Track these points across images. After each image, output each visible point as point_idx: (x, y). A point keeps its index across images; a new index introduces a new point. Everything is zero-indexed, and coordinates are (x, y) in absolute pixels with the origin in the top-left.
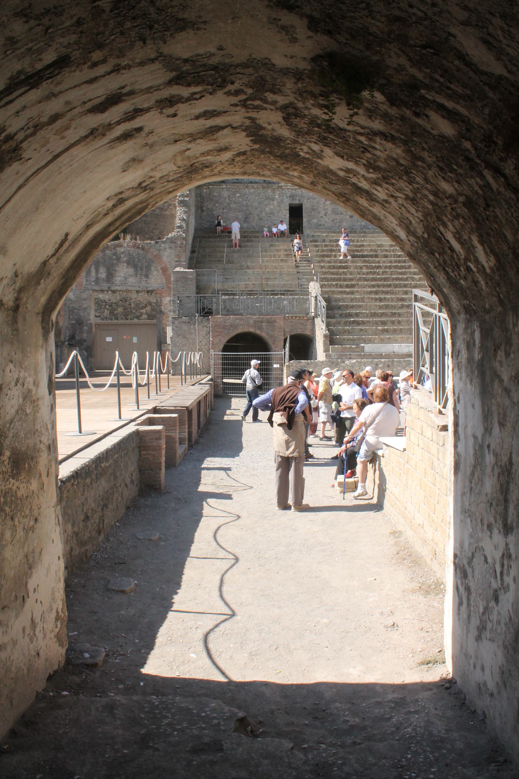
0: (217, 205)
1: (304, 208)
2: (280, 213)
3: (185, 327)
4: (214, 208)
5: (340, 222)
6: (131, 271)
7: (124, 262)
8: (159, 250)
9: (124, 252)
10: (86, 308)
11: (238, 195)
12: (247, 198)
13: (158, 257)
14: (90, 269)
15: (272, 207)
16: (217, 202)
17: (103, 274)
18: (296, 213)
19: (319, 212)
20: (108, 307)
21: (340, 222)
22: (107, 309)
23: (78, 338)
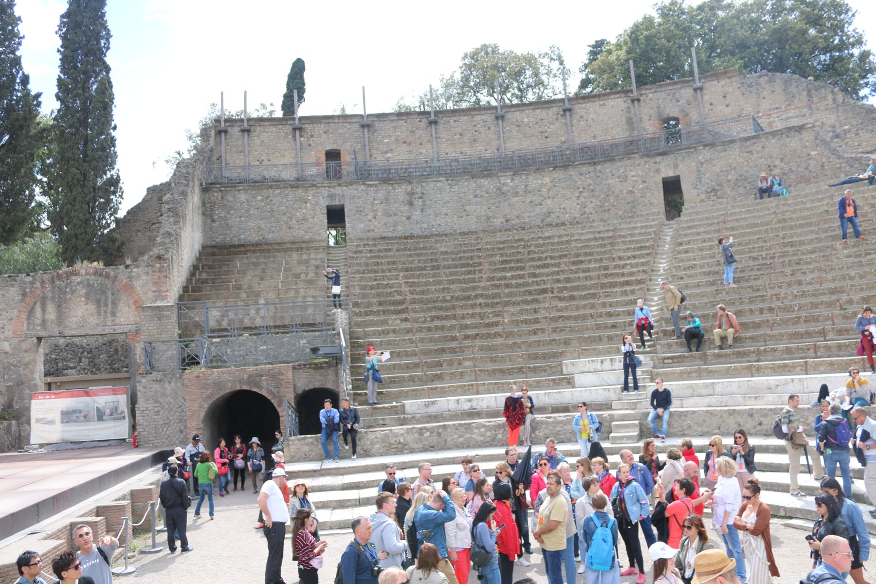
0: (232, 212)
1: (346, 210)
2: (316, 219)
3: (156, 387)
4: (228, 216)
5: (395, 226)
6: (92, 307)
7: (80, 296)
8: (130, 278)
9: (78, 283)
11: (260, 198)
12: (271, 201)
13: (129, 288)
15: (304, 211)
16: (232, 208)
17: (51, 314)
18: (336, 216)
19: (367, 215)
20: (86, 354)
21: (395, 226)
22: (86, 357)
23: (16, 406)
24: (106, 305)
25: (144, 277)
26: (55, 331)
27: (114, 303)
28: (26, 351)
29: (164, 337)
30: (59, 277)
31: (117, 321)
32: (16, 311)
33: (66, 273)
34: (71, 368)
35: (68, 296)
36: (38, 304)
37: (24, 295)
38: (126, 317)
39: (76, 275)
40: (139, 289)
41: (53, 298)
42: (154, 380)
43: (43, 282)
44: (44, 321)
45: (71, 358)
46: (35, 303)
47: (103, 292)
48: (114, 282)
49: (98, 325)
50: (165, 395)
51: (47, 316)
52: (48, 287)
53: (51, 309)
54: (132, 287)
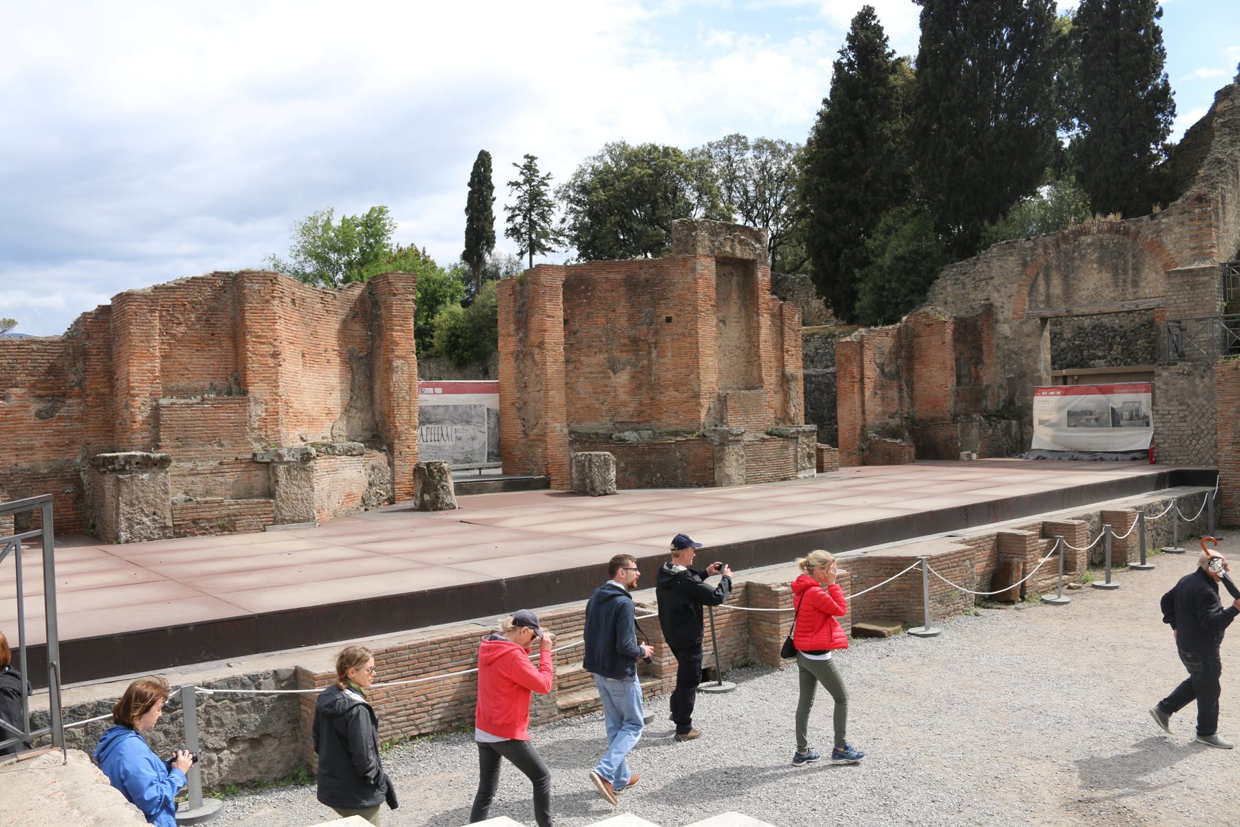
3: (1182, 383)
6: (1107, 276)
7: (1092, 262)
8: (1158, 232)
9: (1089, 245)
10: (1030, 351)
14: (1035, 280)
17: (1057, 289)
22: (1119, 344)
24: (1125, 272)
25: (1177, 230)
26: (1061, 309)
27: (1135, 269)
28: (1028, 335)
29: (1199, 313)
30: (1065, 238)
31: (1141, 293)
32: (1015, 285)
33: (1073, 232)
34: (1100, 358)
35: (1077, 263)
36: (1041, 275)
37: (1025, 264)
38: (1153, 287)
39: (1085, 234)
40: (1170, 246)
41: (1058, 267)
42: (1179, 374)
43: (1046, 247)
44: (1048, 297)
45: (1100, 345)
46: (1038, 274)
47: (1121, 255)
48: (1135, 239)
49: (1115, 299)
50: (1194, 394)
51: (1052, 291)
52: (1051, 251)
53: (1056, 280)
54: (1160, 245)
